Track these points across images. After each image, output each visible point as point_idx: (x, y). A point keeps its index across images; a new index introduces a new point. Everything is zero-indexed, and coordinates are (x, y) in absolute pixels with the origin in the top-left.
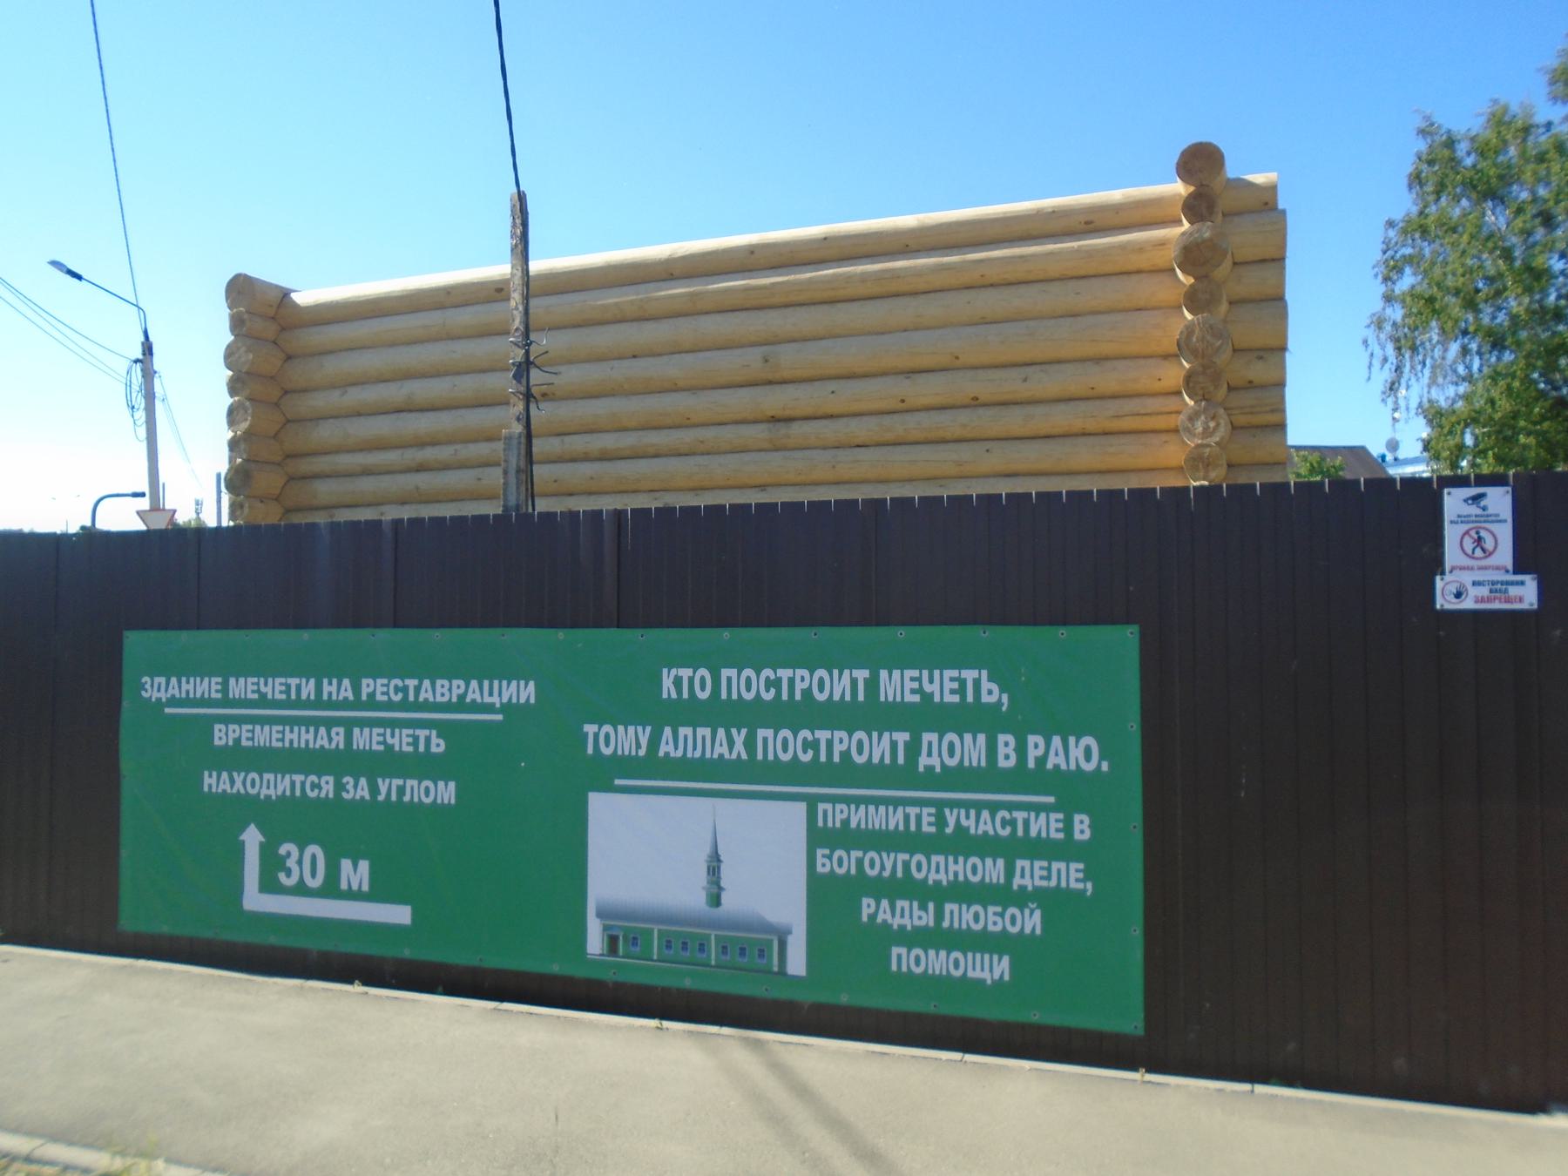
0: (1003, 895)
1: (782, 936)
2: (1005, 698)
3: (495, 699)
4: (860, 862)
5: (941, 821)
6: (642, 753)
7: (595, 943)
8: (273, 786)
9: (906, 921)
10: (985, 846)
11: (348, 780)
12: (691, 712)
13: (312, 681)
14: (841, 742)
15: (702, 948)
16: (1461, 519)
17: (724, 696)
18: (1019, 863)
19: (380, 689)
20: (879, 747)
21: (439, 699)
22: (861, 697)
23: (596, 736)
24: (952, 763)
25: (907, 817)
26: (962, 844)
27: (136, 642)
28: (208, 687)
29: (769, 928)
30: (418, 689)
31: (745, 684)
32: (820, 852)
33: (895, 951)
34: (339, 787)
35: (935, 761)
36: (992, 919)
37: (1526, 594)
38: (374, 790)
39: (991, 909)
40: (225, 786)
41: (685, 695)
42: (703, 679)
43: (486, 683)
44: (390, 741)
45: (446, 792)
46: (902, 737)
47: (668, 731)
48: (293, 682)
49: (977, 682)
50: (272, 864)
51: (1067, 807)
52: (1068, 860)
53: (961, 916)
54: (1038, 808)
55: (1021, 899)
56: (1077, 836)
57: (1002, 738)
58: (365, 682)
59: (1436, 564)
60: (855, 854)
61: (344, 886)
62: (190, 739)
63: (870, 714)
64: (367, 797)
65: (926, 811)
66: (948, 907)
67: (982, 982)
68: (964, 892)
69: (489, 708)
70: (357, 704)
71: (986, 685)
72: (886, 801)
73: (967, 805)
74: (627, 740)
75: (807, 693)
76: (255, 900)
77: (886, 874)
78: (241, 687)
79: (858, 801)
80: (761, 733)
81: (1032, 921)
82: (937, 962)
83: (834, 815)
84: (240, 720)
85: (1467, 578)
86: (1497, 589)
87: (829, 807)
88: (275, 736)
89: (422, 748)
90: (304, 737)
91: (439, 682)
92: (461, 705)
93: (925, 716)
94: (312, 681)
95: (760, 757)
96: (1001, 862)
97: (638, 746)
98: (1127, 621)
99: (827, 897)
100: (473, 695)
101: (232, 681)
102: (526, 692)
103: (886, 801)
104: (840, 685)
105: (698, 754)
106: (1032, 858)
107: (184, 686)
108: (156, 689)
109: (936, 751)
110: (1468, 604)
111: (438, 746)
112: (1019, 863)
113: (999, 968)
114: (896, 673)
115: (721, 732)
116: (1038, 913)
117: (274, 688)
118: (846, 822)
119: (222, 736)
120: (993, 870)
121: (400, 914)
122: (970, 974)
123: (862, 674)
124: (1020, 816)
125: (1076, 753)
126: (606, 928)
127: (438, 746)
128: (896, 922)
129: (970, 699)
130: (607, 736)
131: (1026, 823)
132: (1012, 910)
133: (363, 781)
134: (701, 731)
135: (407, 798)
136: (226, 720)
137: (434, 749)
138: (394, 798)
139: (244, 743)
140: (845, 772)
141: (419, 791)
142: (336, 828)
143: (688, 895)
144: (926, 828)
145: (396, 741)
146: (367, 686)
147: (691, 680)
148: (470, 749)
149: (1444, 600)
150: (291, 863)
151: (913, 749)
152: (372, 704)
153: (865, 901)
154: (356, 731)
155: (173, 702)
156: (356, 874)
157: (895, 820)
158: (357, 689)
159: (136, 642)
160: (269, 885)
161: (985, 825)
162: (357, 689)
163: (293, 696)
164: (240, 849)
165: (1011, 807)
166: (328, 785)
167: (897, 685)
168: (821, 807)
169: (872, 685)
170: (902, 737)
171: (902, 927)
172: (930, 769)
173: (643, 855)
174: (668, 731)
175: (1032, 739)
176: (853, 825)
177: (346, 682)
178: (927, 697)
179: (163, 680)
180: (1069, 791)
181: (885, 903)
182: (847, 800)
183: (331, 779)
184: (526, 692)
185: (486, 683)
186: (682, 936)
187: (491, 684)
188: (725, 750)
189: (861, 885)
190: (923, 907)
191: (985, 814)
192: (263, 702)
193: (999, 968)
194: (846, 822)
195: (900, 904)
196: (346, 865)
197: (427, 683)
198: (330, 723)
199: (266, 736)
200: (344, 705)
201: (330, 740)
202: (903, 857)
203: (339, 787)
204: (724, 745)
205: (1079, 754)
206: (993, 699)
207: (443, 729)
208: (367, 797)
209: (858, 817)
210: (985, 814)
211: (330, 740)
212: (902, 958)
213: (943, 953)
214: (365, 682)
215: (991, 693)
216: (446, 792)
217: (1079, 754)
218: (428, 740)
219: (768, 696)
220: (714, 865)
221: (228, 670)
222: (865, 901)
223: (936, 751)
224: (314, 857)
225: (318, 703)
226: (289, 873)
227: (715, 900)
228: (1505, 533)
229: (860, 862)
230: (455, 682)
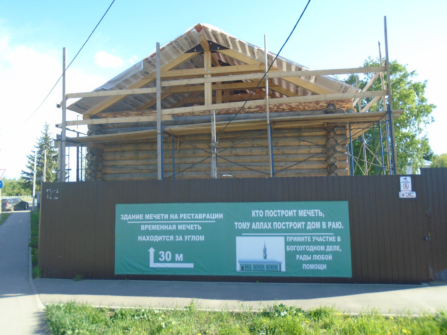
0: (324, 253)
2: (323, 215)
3: (213, 218)
4: (296, 248)
5: (312, 239)
6: (248, 228)
7: (238, 268)
8: (157, 239)
9: (306, 259)
10: (321, 243)
11: (177, 236)
13: (167, 215)
14: (291, 224)
16: (403, 182)
17: (266, 216)
18: (327, 246)
19: (184, 216)
20: (299, 225)
21: (200, 218)
22: (295, 215)
23: (237, 225)
24: (314, 228)
25: (305, 239)
26: (316, 243)
27: (119, 207)
28: (140, 217)
29: (278, 262)
30: (194, 216)
31: (270, 213)
32: (287, 246)
33: (304, 265)
34: (175, 238)
36: (322, 257)
37: (414, 195)
38: (184, 238)
39: (322, 255)
40: (144, 239)
41: (257, 216)
42: (261, 213)
43: (211, 214)
44: (187, 227)
45: (202, 238)
47: (254, 223)
48: (162, 215)
49: (318, 212)
51: (336, 235)
52: (337, 245)
54: (330, 236)
55: (328, 253)
56: (338, 241)
57: (323, 223)
58: (181, 215)
59: (399, 190)
60: (295, 246)
61: (176, 260)
62: (135, 229)
63: (297, 219)
64: (182, 240)
65: (309, 237)
67: (321, 270)
68: (317, 253)
69: (212, 220)
70: (179, 219)
71: (320, 213)
72: (301, 236)
73: (317, 236)
74: (244, 225)
75: (284, 215)
76: (152, 264)
77: (301, 250)
78: (147, 217)
79: (295, 236)
80: (274, 223)
81: (330, 257)
82: (312, 267)
83: (290, 239)
84: (148, 224)
85: (404, 192)
86: (409, 194)
87: (289, 237)
88: (158, 227)
89: (196, 229)
90: (165, 227)
91: (199, 214)
92: (205, 219)
93: (308, 219)
94: (167, 215)
95: (274, 228)
96: (324, 246)
97: (247, 226)
98: (346, 200)
99: (289, 256)
100: (208, 216)
101: (146, 215)
102: (221, 216)
103: (301, 236)
104: (290, 213)
105: (261, 228)
107: (133, 217)
108: (125, 217)
109: (310, 226)
110: (405, 197)
111: (200, 228)
112: (327, 246)
113: (325, 267)
114: (302, 211)
115: (266, 223)
116: (331, 256)
117: (157, 216)
118: (293, 240)
119: (143, 228)
120: (322, 248)
121: (191, 265)
122: (319, 268)
123: (295, 211)
124: (327, 237)
125: (337, 225)
126: (241, 265)
127: (200, 228)
128: (303, 259)
129: (317, 215)
130: (240, 225)
131: (328, 238)
132: (326, 255)
133: (181, 236)
134: (261, 223)
135: (192, 240)
136: (144, 224)
137: (199, 229)
138: (189, 240)
139: (149, 229)
140: (292, 230)
142: (174, 247)
144: (309, 241)
145: (189, 227)
146: (181, 215)
147: (259, 213)
148: (207, 229)
149: (401, 196)
150: (162, 256)
151: (306, 225)
152: (183, 219)
153: (297, 256)
154: (179, 225)
155: (130, 220)
157: (303, 239)
158: (179, 216)
159: (119, 207)
161: (320, 239)
162: (179, 216)
163: (162, 218)
164: (149, 253)
165: (325, 236)
166: (172, 238)
168: (287, 237)
169: (297, 213)
171: (305, 260)
172: (309, 229)
174: (254, 223)
175: (329, 223)
176: (294, 241)
177: (176, 215)
178: (308, 215)
179: (127, 215)
180: (336, 232)
181: (301, 256)
182: (293, 236)
183: (173, 236)
184: (221, 216)
185: (211, 214)
186: (258, 266)
187: (211, 215)
189: (296, 252)
190: (309, 256)
191: (320, 237)
192: (154, 219)
193: (323, 267)
194: (293, 240)
195: (304, 256)
196: (177, 255)
197: (197, 215)
198: (172, 224)
199: (154, 227)
200: (176, 220)
201: (172, 228)
202: (304, 246)
203: (175, 238)
205: (338, 225)
206: (321, 215)
207: (201, 224)
208: (182, 240)
209: (295, 239)
210: (320, 237)
211: (172, 228)
212: (305, 266)
213: (313, 265)
214: (181, 215)
215: (321, 214)
216: (202, 238)
217: (338, 225)
218: (197, 227)
219: (276, 216)
220: (265, 251)
221: (144, 213)
222: (297, 256)
223: (310, 226)
224: (168, 254)
225: (169, 219)
226: (162, 258)
227: (265, 257)
229: (296, 248)
230: (203, 214)
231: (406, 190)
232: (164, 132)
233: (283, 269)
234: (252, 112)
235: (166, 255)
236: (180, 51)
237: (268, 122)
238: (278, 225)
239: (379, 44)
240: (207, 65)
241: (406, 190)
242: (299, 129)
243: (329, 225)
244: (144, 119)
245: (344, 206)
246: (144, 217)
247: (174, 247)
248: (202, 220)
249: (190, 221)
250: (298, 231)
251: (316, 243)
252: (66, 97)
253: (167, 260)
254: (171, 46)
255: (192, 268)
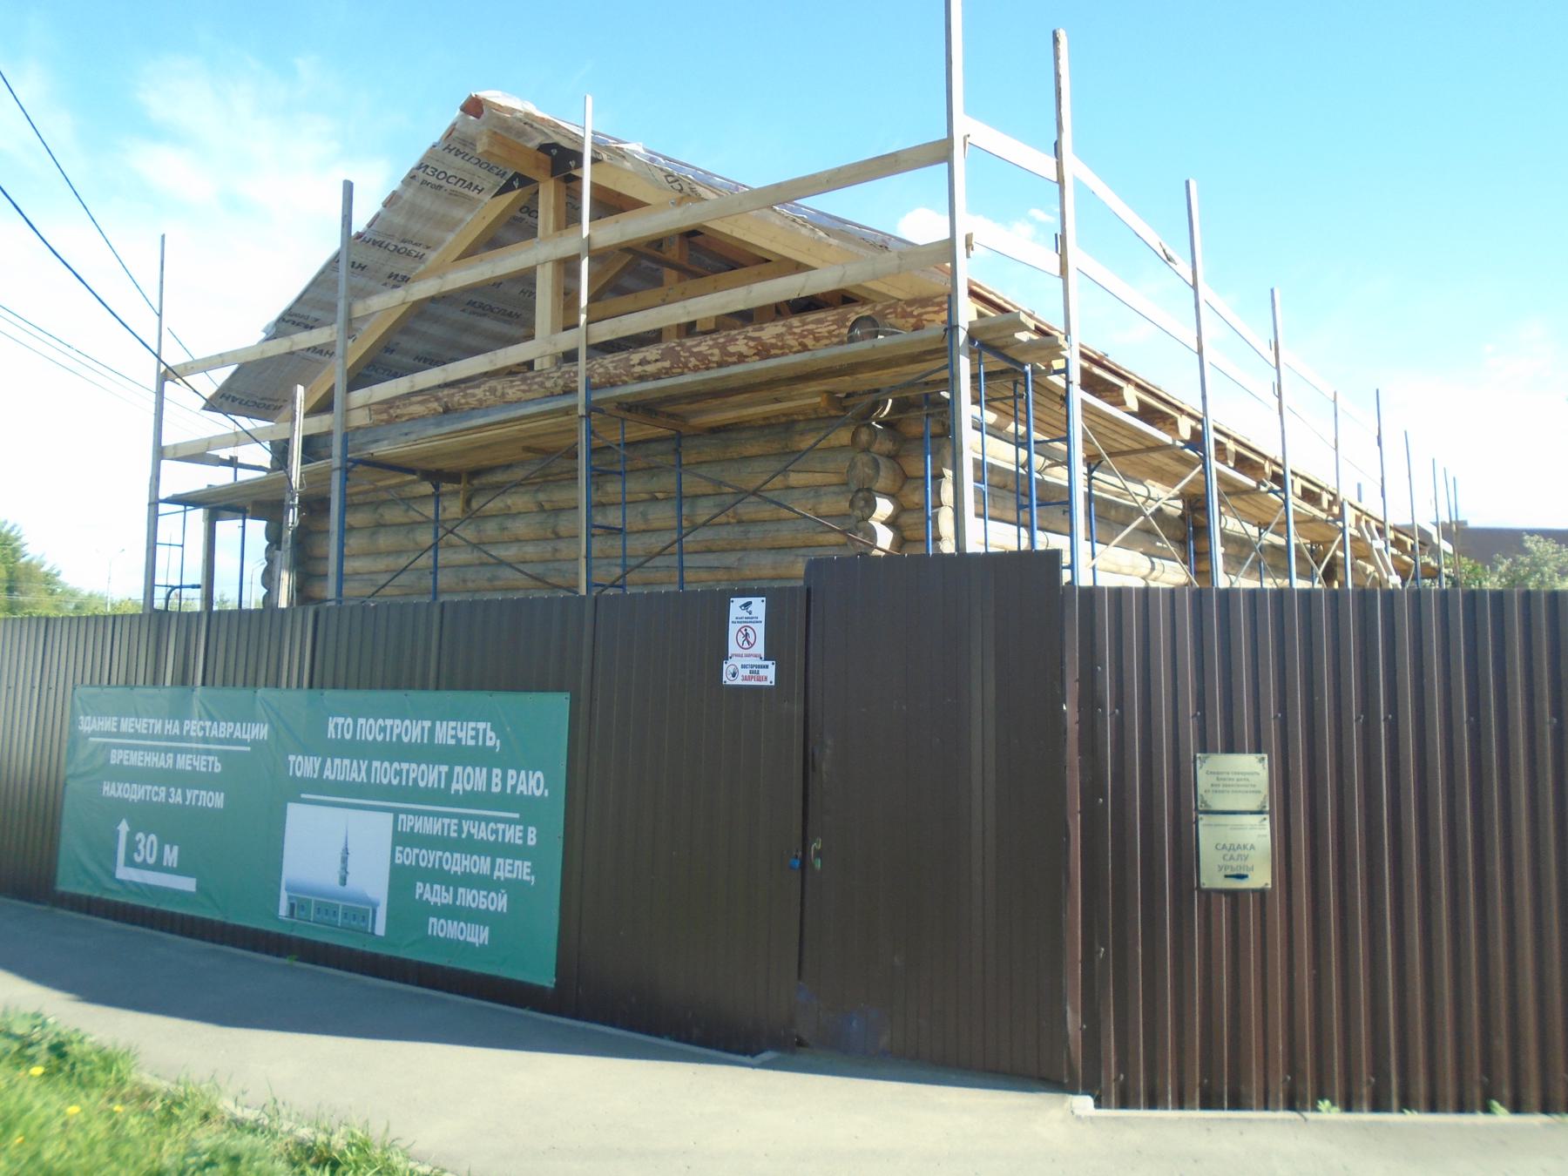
1: (374, 906)
5: (460, 831)
7: (283, 911)
15: (335, 914)
16: (739, 620)
20: (430, 776)
24: (468, 788)
31: (370, 729)
32: (399, 848)
33: (432, 920)
34: (168, 795)
35: (459, 787)
37: (769, 675)
40: (113, 792)
46: (444, 769)
50: (132, 847)
59: (724, 655)
60: (416, 851)
63: (428, 753)
66: (461, 890)
69: (242, 742)
78: (127, 725)
81: (501, 903)
83: (408, 823)
86: (754, 670)
92: (230, 741)
99: (401, 879)
102: (261, 731)
104: (414, 731)
106: (506, 857)
110: (739, 681)
118: (412, 828)
120: (482, 865)
121: (188, 884)
124: (501, 826)
126: (290, 898)
128: (433, 900)
132: (493, 894)
150: (141, 847)
156: (172, 856)
160: (130, 862)
161: (482, 833)
164: (116, 834)
167: (446, 732)
169: (432, 730)
170: (444, 769)
172: (457, 791)
175: (511, 772)
178: (459, 740)
180: (526, 808)
184: (261, 731)
188: (354, 775)
190: (447, 891)
193: (479, 936)
194: (412, 828)
196: (167, 847)
202: (440, 853)
203: (168, 795)
205: (532, 784)
215: (492, 740)
216: (218, 800)
217: (532, 784)
220: (344, 860)
227: (344, 881)
228: (760, 629)
231: (747, 660)
233: (380, 930)
234: (656, 376)
236: (474, 194)
237: (581, 411)
239: (1056, 40)
240: (546, 228)
242: (785, 426)
243: (510, 782)
246: (118, 727)
248: (220, 741)
252: (168, 374)
253: (151, 861)
254: (416, 183)
255: (190, 893)
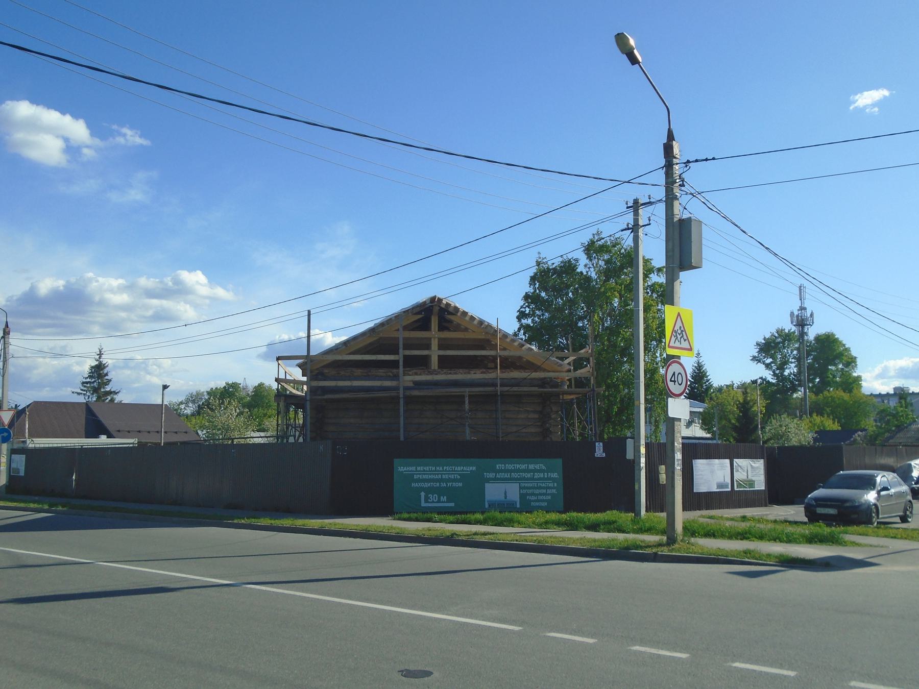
7: (487, 506)
8: (427, 485)
10: (543, 488)
12: (501, 471)
20: (529, 475)
26: (541, 488)
27: (396, 461)
28: (414, 468)
31: (510, 467)
36: (544, 498)
37: (604, 455)
45: (460, 485)
53: (541, 497)
68: (541, 494)
74: (492, 475)
76: (423, 504)
78: (419, 468)
81: (549, 497)
99: (522, 496)
104: (523, 467)
108: (401, 469)
109: (537, 475)
117: (427, 468)
119: (415, 477)
120: (544, 491)
121: (452, 504)
140: (524, 479)
141: (455, 484)
142: (440, 492)
143: (503, 498)
159: (396, 461)
166: (438, 484)
167: (531, 467)
173: (493, 492)
184: (474, 468)
187: (468, 467)
189: (527, 494)
199: (424, 477)
204: (507, 476)
205: (555, 475)
216: (460, 485)
217: (555, 475)
223: (537, 475)
231: (599, 452)
232: (405, 397)
233: (518, 506)
235: (433, 497)
238: (514, 475)
241: (599, 452)
244: (388, 383)
245: (559, 462)
247: (440, 492)
249: (453, 471)
250: (528, 479)
251: (541, 488)
